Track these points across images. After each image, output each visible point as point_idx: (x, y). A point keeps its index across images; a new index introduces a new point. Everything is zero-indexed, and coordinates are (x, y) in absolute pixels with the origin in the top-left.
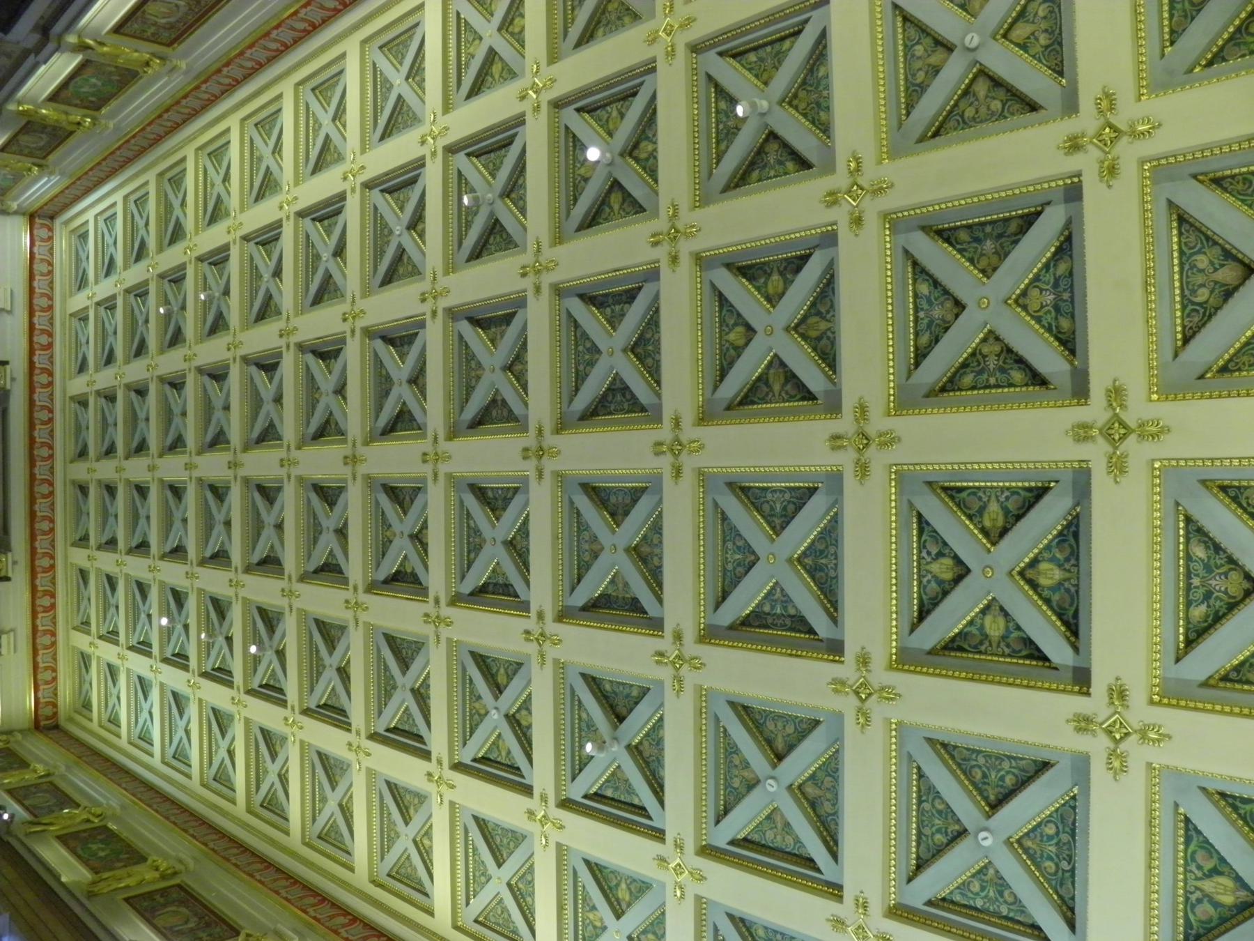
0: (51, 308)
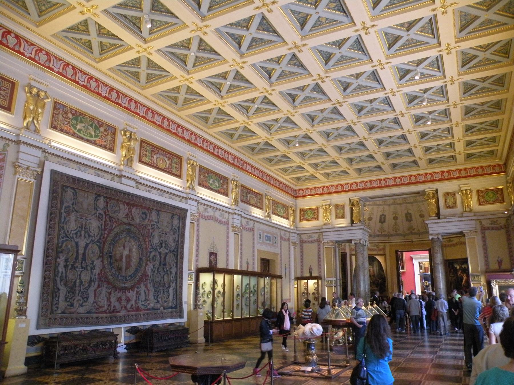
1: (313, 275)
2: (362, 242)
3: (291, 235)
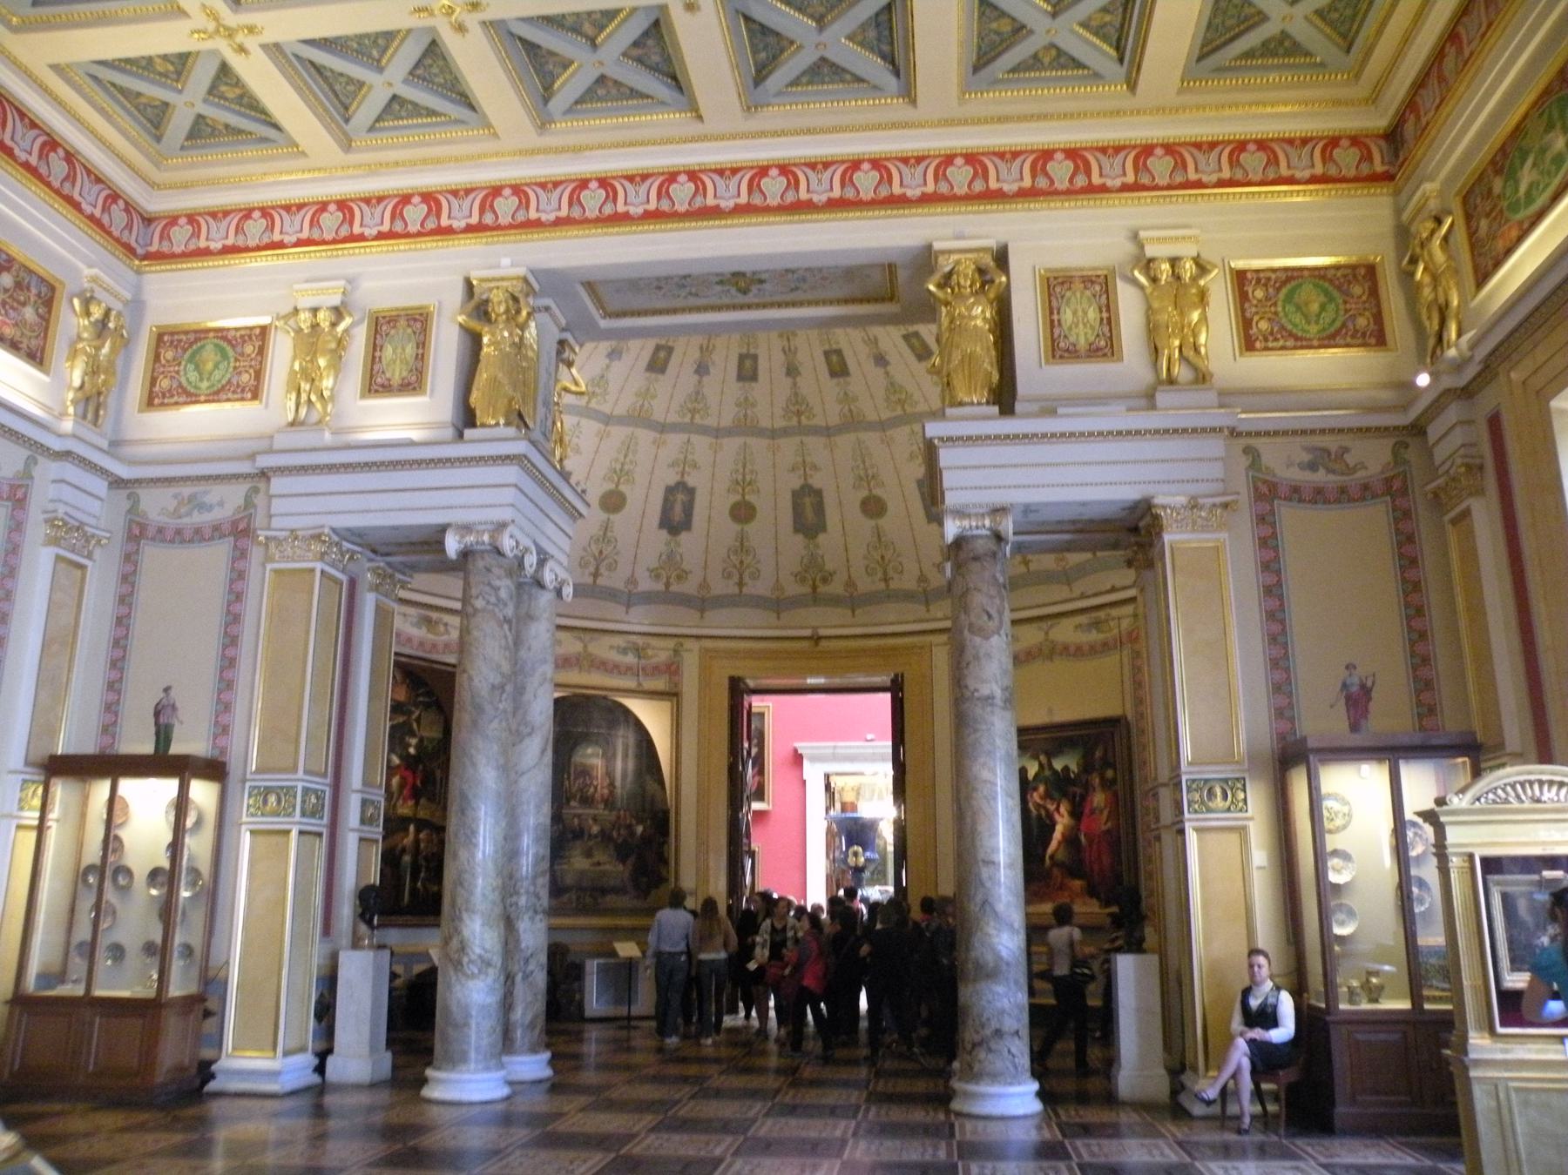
0: (343, 205)
1: (176, 749)
2: (507, 544)
3: (47, 470)
